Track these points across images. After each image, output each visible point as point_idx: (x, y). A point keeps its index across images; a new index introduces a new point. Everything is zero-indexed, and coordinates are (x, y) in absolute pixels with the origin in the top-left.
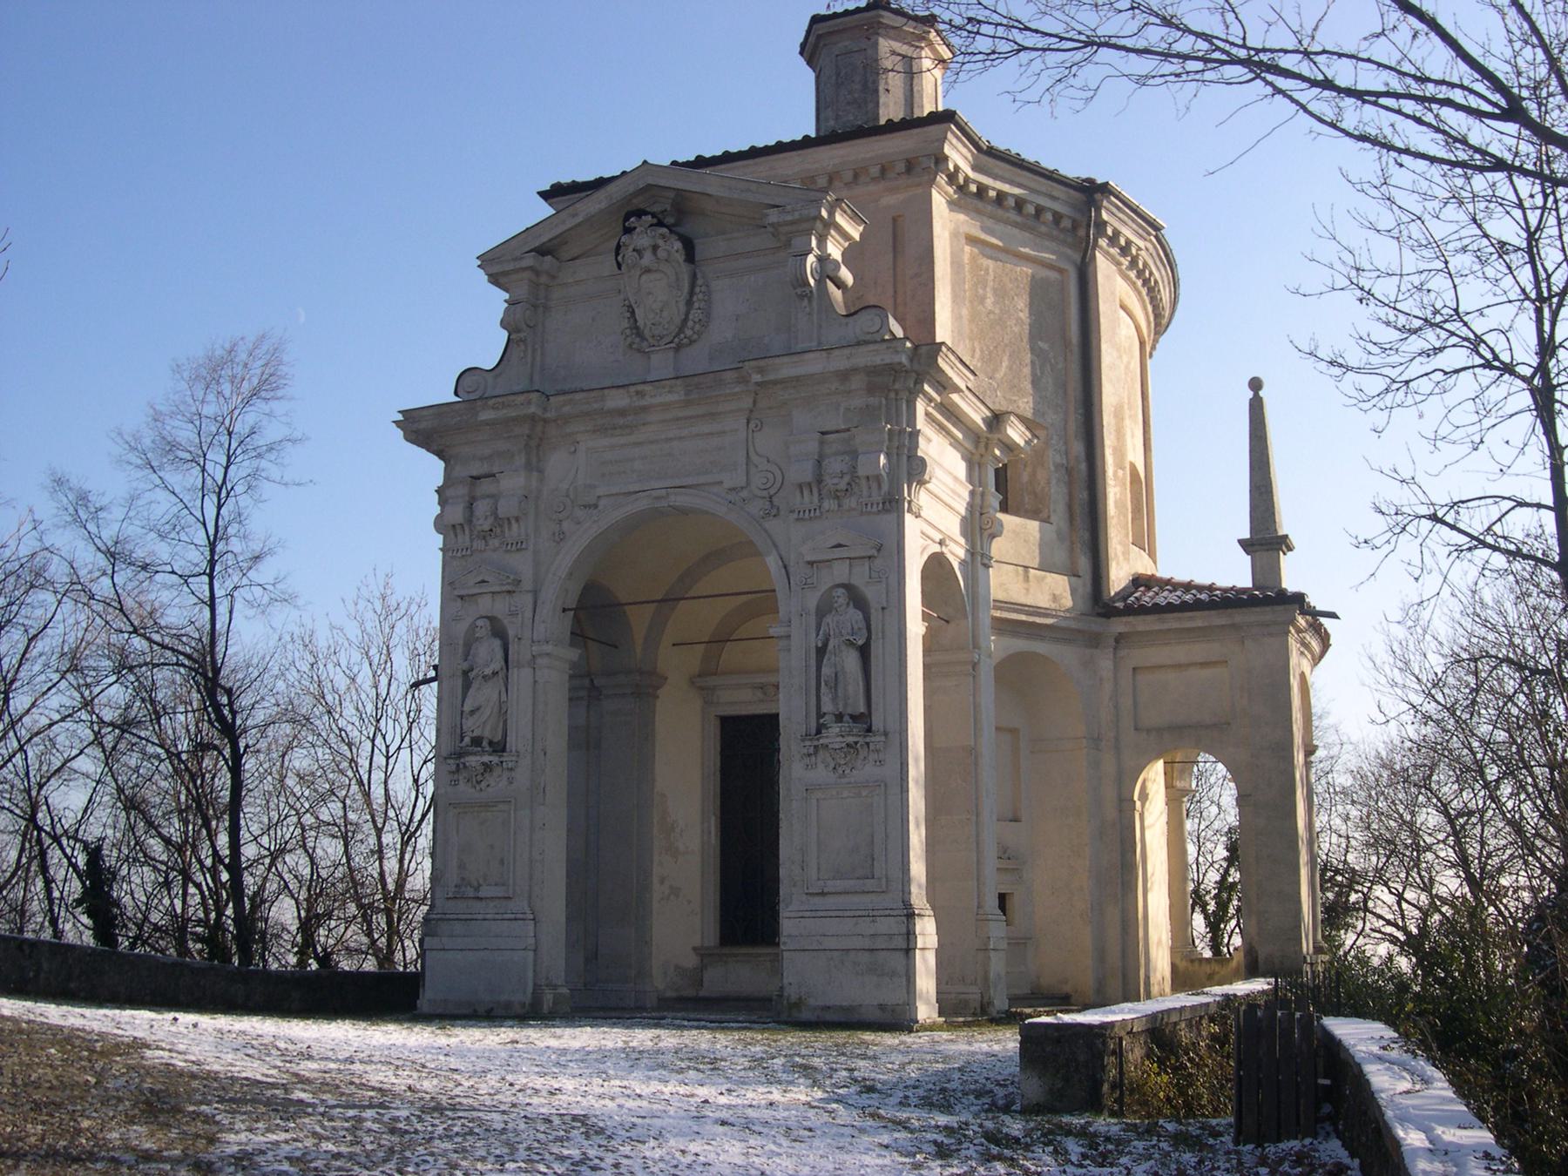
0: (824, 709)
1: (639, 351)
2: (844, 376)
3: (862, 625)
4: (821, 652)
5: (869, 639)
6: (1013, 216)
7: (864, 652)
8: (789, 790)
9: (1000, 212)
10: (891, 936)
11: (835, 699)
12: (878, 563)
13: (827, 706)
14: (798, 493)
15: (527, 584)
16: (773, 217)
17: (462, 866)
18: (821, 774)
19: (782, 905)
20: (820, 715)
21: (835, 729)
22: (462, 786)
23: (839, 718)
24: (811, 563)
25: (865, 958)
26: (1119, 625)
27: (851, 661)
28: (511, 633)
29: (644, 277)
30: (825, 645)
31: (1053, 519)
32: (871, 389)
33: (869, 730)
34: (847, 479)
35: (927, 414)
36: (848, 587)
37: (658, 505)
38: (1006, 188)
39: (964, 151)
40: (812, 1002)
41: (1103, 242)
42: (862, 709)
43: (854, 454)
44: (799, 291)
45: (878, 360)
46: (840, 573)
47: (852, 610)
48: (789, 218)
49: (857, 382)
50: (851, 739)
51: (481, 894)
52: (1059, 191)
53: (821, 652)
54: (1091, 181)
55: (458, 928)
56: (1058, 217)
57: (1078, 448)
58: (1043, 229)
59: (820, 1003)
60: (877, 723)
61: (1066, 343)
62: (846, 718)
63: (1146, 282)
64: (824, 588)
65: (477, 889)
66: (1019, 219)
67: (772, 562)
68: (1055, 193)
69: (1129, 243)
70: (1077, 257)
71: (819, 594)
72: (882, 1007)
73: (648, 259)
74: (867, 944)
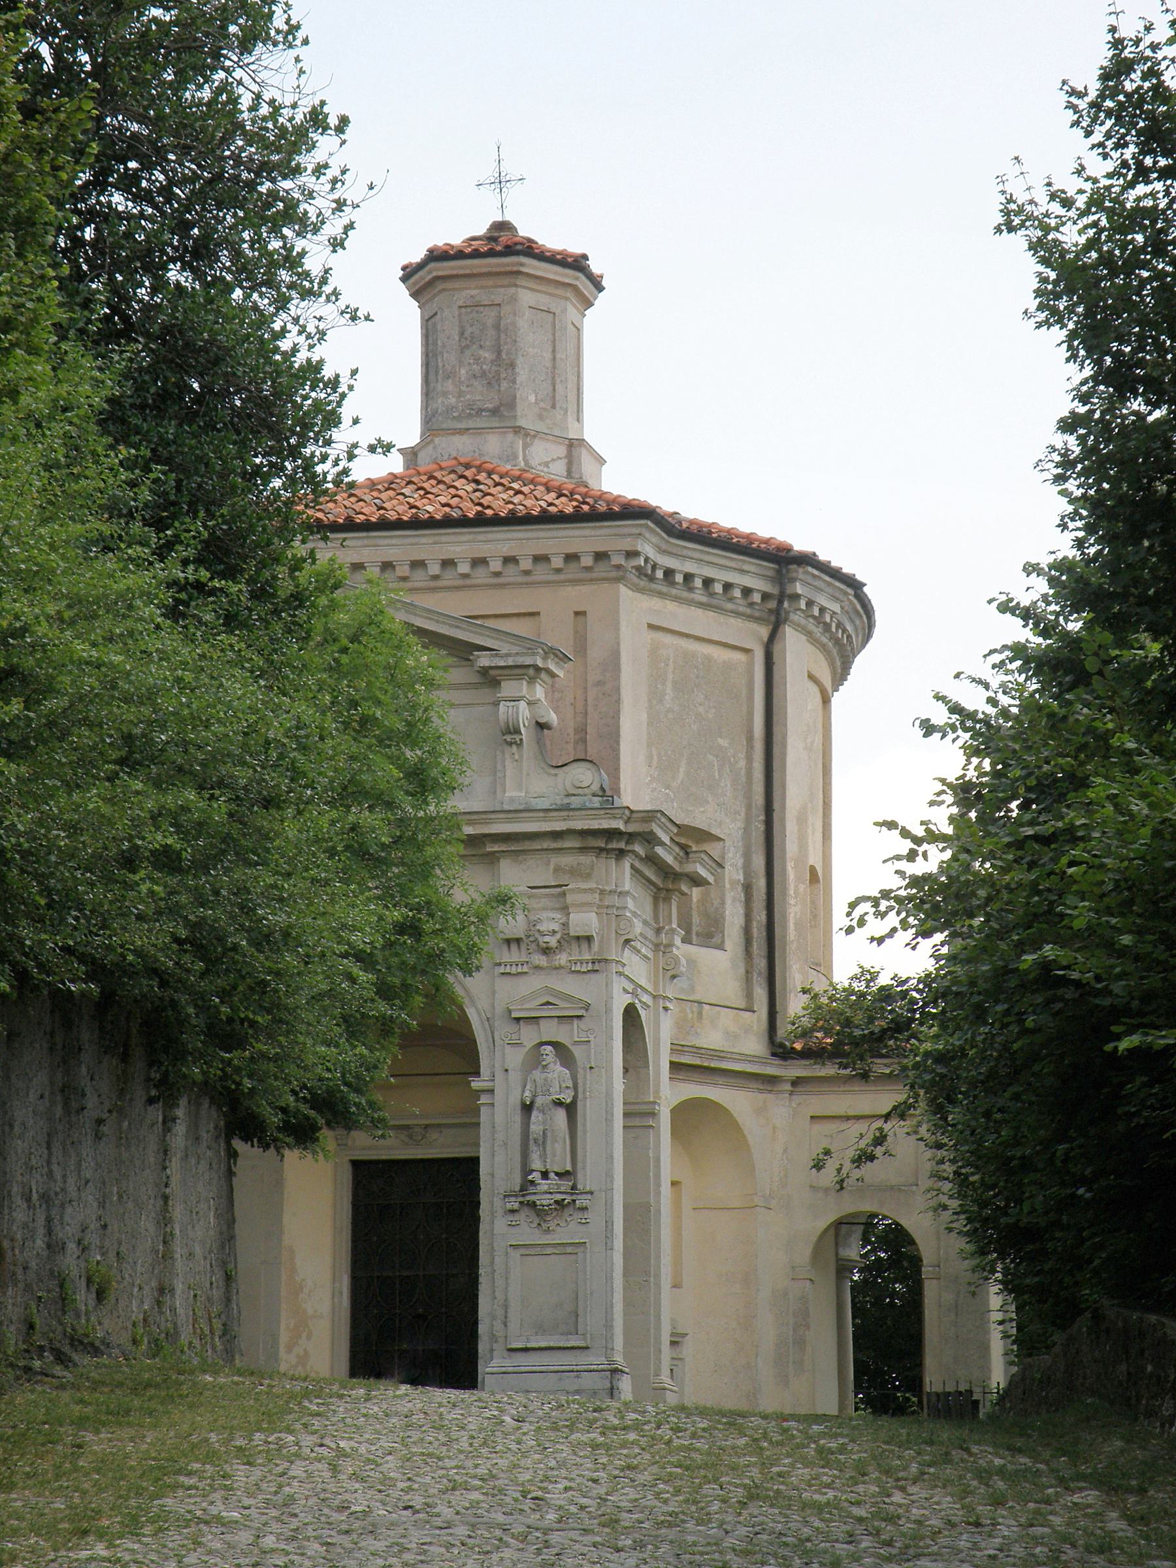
0: (534, 1167)
2: (557, 835)
3: (570, 1084)
4: (527, 1108)
5: (575, 1098)
6: (700, 596)
7: (571, 1109)
8: (491, 1244)
9: (685, 594)
11: (543, 1157)
12: (583, 1024)
13: (537, 1164)
14: (505, 947)
16: (484, 660)
18: (526, 1231)
19: (481, 1362)
20: (526, 1171)
21: (544, 1185)
23: (545, 1175)
24: (518, 1019)
26: (797, 1070)
27: (561, 1115)
30: (532, 1103)
31: (728, 945)
32: (583, 850)
33: (574, 1187)
34: (558, 936)
35: (632, 866)
36: (555, 1045)
38: (690, 567)
39: (654, 539)
41: (795, 617)
42: (569, 1168)
43: (565, 909)
44: (508, 738)
45: (595, 825)
46: (551, 1031)
47: (559, 1068)
48: (502, 663)
50: (559, 1197)
52: (750, 564)
53: (527, 1108)
54: (788, 549)
56: (747, 592)
57: (759, 861)
58: (730, 606)
60: (586, 1181)
61: (750, 739)
62: (552, 1175)
63: (837, 642)
64: (529, 1044)
66: (704, 599)
67: (471, 1013)
68: (746, 567)
69: (822, 610)
70: (764, 632)
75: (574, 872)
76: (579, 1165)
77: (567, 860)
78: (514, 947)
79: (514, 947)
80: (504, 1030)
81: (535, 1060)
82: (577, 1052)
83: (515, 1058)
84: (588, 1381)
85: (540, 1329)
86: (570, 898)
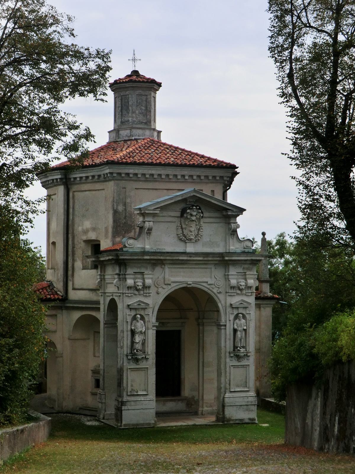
1: (182, 241)
10: (252, 402)
15: (151, 306)
17: (132, 386)
22: (131, 363)
25: (245, 407)
28: (146, 319)
29: (190, 222)
32: (250, 264)
37: (188, 286)
40: (232, 418)
43: (246, 280)
46: (241, 311)
49: (248, 262)
51: (139, 393)
55: (133, 403)
59: (234, 418)
65: (137, 392)
71: (234, 315)
72: (250, 419)
73: (194, 218)
74: (246, 404)
75: (248, 269)
76: (247, 345)
77: (246, 266)
78: (232, 289)
79: (232, 289)
80: (229, 310)
81: (236, 317)
82: (247, 316)
83: (232, 317)
84: (250, 399)
85: (238, 386)
86: (247, 276)
